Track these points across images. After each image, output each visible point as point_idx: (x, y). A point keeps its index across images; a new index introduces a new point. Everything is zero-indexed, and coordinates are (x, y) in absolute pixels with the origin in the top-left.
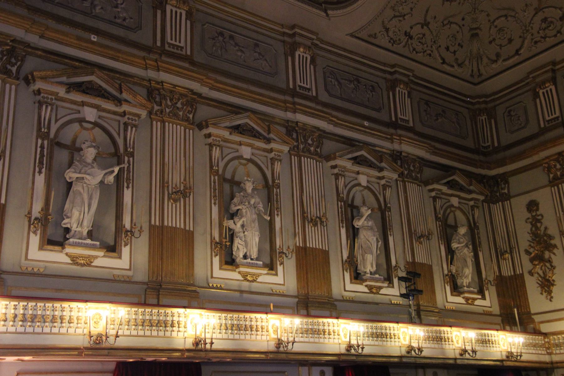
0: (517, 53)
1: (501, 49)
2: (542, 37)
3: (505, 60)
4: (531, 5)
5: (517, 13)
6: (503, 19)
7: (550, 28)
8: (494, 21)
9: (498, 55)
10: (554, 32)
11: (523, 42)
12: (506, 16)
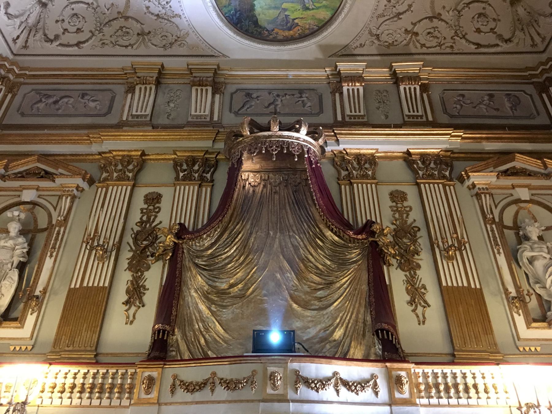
0: (78, 44)
1: (63, 33)
2: (111, 42)
3: (61, 45)
7: (124, 38)
9: (57, 37)
10: (127, 43)
11: (90, 38)
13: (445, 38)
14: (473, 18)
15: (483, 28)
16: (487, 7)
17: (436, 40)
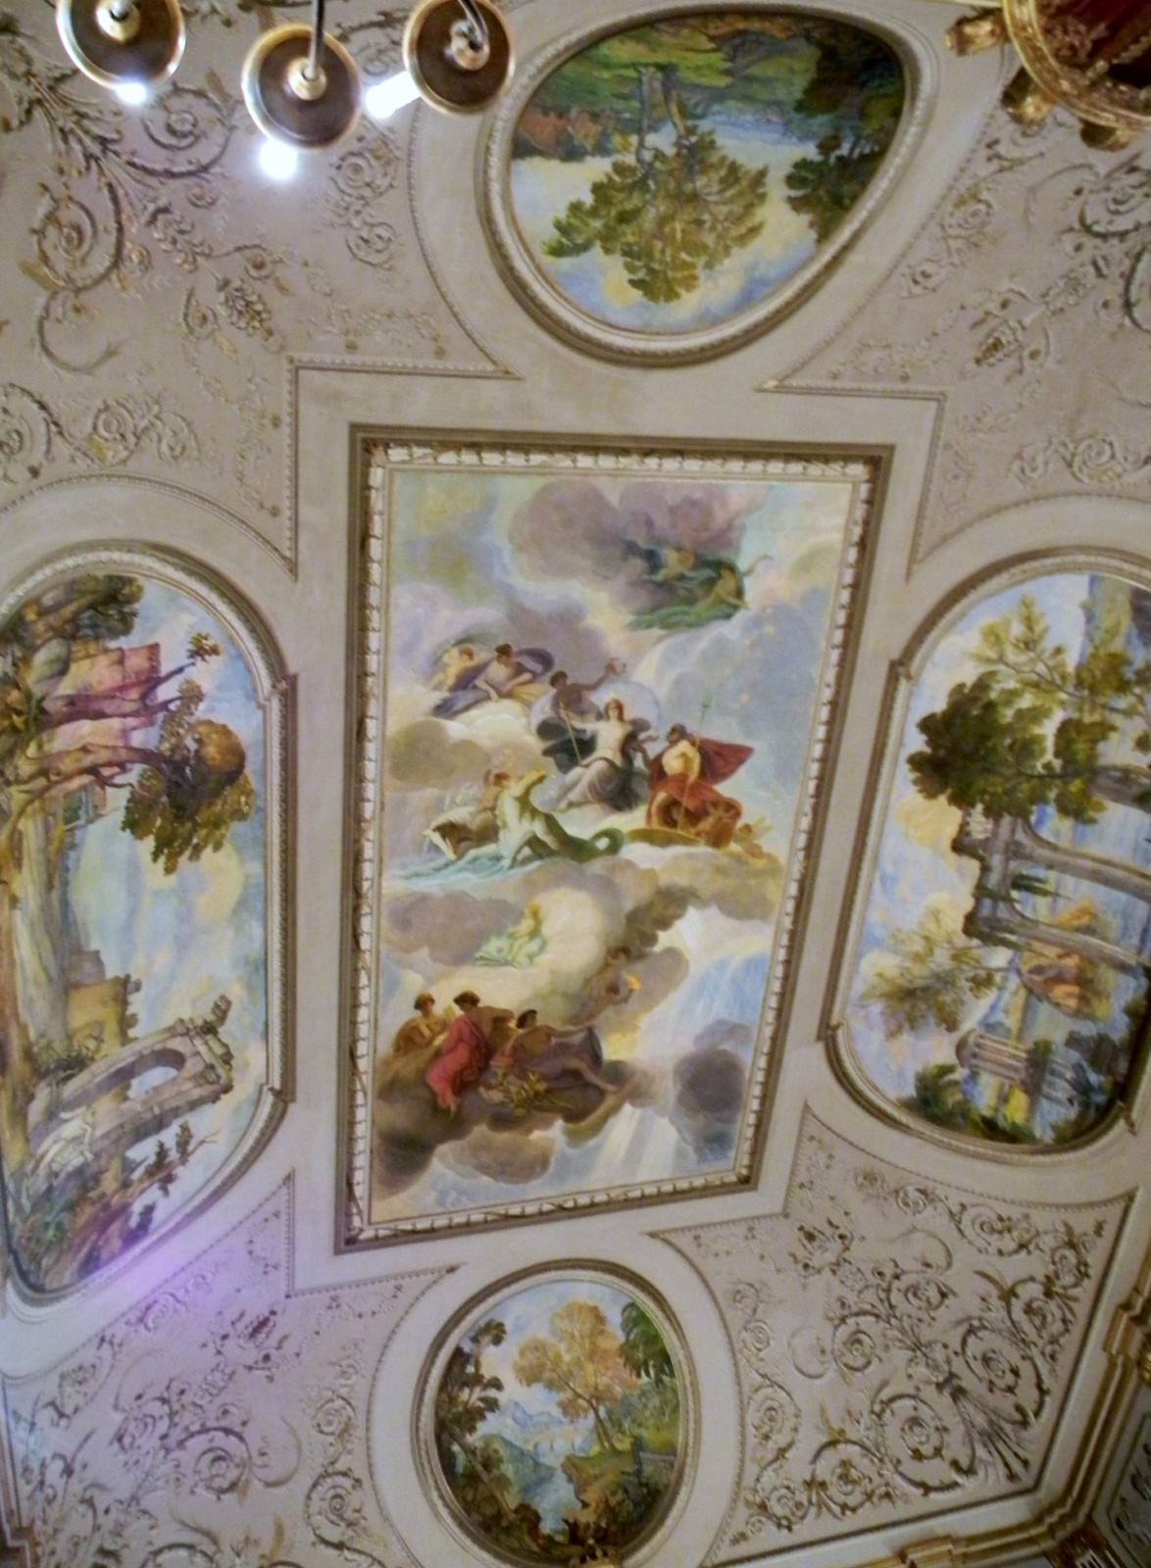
4: (257, 1543)
5: (219, 1551)
6: (183, 1553)
8: (160, 1551)
12: (191, 1547)
15: (927, 1450)
16: (921, 1406)
17: (858, 1489)
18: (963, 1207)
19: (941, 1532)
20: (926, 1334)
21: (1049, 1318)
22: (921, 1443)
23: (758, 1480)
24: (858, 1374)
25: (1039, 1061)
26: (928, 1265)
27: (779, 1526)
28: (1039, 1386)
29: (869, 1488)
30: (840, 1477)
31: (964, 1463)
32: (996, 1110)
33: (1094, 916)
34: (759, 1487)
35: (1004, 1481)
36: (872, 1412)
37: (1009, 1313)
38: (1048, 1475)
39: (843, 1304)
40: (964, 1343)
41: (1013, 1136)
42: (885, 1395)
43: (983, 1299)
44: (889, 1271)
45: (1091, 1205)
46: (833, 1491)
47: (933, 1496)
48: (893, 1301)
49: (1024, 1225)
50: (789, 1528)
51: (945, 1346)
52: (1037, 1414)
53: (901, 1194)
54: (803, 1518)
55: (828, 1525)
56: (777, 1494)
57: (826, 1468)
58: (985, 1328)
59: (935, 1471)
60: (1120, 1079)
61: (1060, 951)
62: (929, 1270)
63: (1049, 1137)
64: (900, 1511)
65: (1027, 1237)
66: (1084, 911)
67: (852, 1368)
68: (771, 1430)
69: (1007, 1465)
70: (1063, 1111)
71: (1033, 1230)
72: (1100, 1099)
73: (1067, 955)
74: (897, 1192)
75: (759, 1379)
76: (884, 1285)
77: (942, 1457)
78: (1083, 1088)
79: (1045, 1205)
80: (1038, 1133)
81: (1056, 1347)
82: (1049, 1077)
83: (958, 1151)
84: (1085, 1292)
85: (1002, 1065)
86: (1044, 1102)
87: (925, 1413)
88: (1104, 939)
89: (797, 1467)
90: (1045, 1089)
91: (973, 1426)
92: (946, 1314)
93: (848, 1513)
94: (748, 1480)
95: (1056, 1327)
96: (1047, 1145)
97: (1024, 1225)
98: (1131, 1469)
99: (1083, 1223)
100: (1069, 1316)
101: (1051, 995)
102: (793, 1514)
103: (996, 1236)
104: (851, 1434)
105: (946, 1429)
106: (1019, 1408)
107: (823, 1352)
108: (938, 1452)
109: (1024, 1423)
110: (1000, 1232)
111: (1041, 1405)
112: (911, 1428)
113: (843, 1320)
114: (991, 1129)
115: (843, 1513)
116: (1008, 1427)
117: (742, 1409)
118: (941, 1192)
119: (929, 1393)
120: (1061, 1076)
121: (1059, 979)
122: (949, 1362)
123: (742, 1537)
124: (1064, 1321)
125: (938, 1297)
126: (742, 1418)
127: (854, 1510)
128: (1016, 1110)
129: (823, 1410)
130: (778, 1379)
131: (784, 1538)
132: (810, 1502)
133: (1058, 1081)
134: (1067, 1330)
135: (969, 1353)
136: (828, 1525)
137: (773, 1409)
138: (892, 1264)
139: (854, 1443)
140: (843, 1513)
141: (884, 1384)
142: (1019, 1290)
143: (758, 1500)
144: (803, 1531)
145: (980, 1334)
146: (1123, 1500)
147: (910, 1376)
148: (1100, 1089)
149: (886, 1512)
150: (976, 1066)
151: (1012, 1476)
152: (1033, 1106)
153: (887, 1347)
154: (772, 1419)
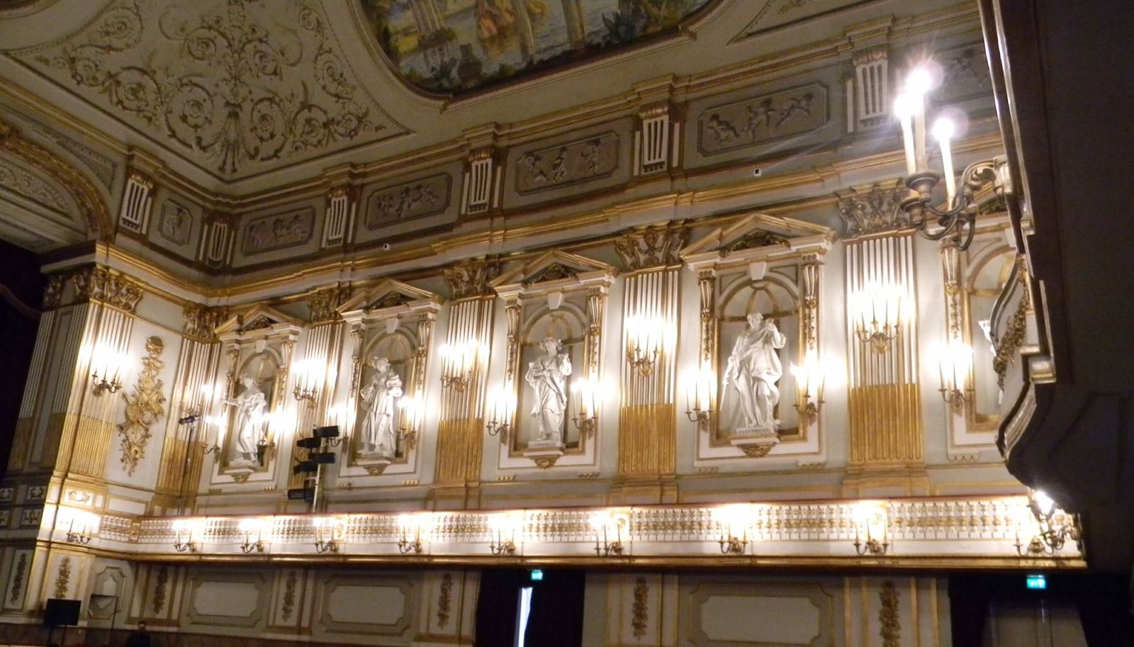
13: (147, 105)
14: (188, 102)
15: (190, 120)
17: (136, 103)
18: (330, 51)
19: (162, 157)
20: (246, 77)
21: (314, 134)
22: (191, 115)
23: (82, 46)
24: (191, 58)
25: (441, 38)
26: (283, 54)
27: (74, 77)
28: (277, 151)
29: (143, 107)
30: (132, 89)
31: (204, 143)
32: (397, 33)
33: (542, 14)
34: (79, 50)
35: (216, 166)
36: (180, 80)
37: (298, 113)
38: (240, 184)
39: (218, 22)
40: (261, 100)
41: (391, 53)
42: (195, 80)
43: (292, 95)
44: (260, 34)
45: (388, 116)
46: (121, 90)
47: (173, 140)
48: (246, 48)
49: (349, 90)
50: (79, 83)
51: (250, 92)
52: (262, 159)
53: (307, 12)
54: (91, 85)
55: (103, 100)
56: (87, 63)
57: (129, 78)
58: (279, 107)
59: (183, 130)
60: (464, 87)
61: (510, 7)
62: (280, 56)
63: (405, 70)
64: (151, 132)
65: (344, 95)
66: (542, 7)
67: (190, 52)
68: (114, 33)
69: (224, 162)
70: (425, 68)
71: (350, 96)
72: (445, 83)
73: (511, 14)
74: (306, 8)
75: (133, 5)
76: (250, 37)
77: (196, 131)
78: (444, 71)
79: (367, 92)
80: (402, 64)
81: (303, 147)
82: (437, 49)
83: (357, 26)
84: (343, 142)
85: (423, 18)
86: (422, 56)
87: (207, 106)
88: (533, 29)
89: (112, 63)
90: (429, 52)
91: (226, 134)
92: (267, 81)
93: (120, 106)
94: (77, 41)
95: (315, 141)
96: (400, 73)
97: (349, 90)
98: (281, 217)
99: (375, 118)
100: (324, 142)
101: (482, 20)
102: (88, 79)
103: (331, 79)
104: (160, 76)
105: (210, 122)
106: (257, 150)
107: (183, 30)
108: (196, 127)
109: (252, 157)
110: (334, 80)
111: (269, 158)
112: (193, 105)
113: (210, 28)
114: (384, 37)
115: (117, 104)
116: (242, 151)
117: (107, 7)
118: (327, 32)
119: (219, 101)
120: (442, 55)
121: (494, 18)
122: (244, 99)
123: (47, 62)
124: (319, 142)
125: (272, 70)
126: (102, 12)
127: (125, 108)
128: (406, 44)
129: (153, 54)
130: (144, 16)
131: (72, 84)
132: (103, 83)
133: (438, 55)
134: (316, 146)
135: (259, 106)
136: (103, 100)
137: (125, 25)
138: (264, 33)
139: (155, 82)
140: (117, 104)
141: (201, 75)
142: (314, 110)
143: (73, 54)
144: (83, 90)
145: (274, 105)
146: (263, 223)
147: (217, 85)
148: (451, 81)
149: (141, 124)
150: (412, 5)
151: (222, 169)
152: (415, 51)
153: (219, 62)
154: (119, 29)
